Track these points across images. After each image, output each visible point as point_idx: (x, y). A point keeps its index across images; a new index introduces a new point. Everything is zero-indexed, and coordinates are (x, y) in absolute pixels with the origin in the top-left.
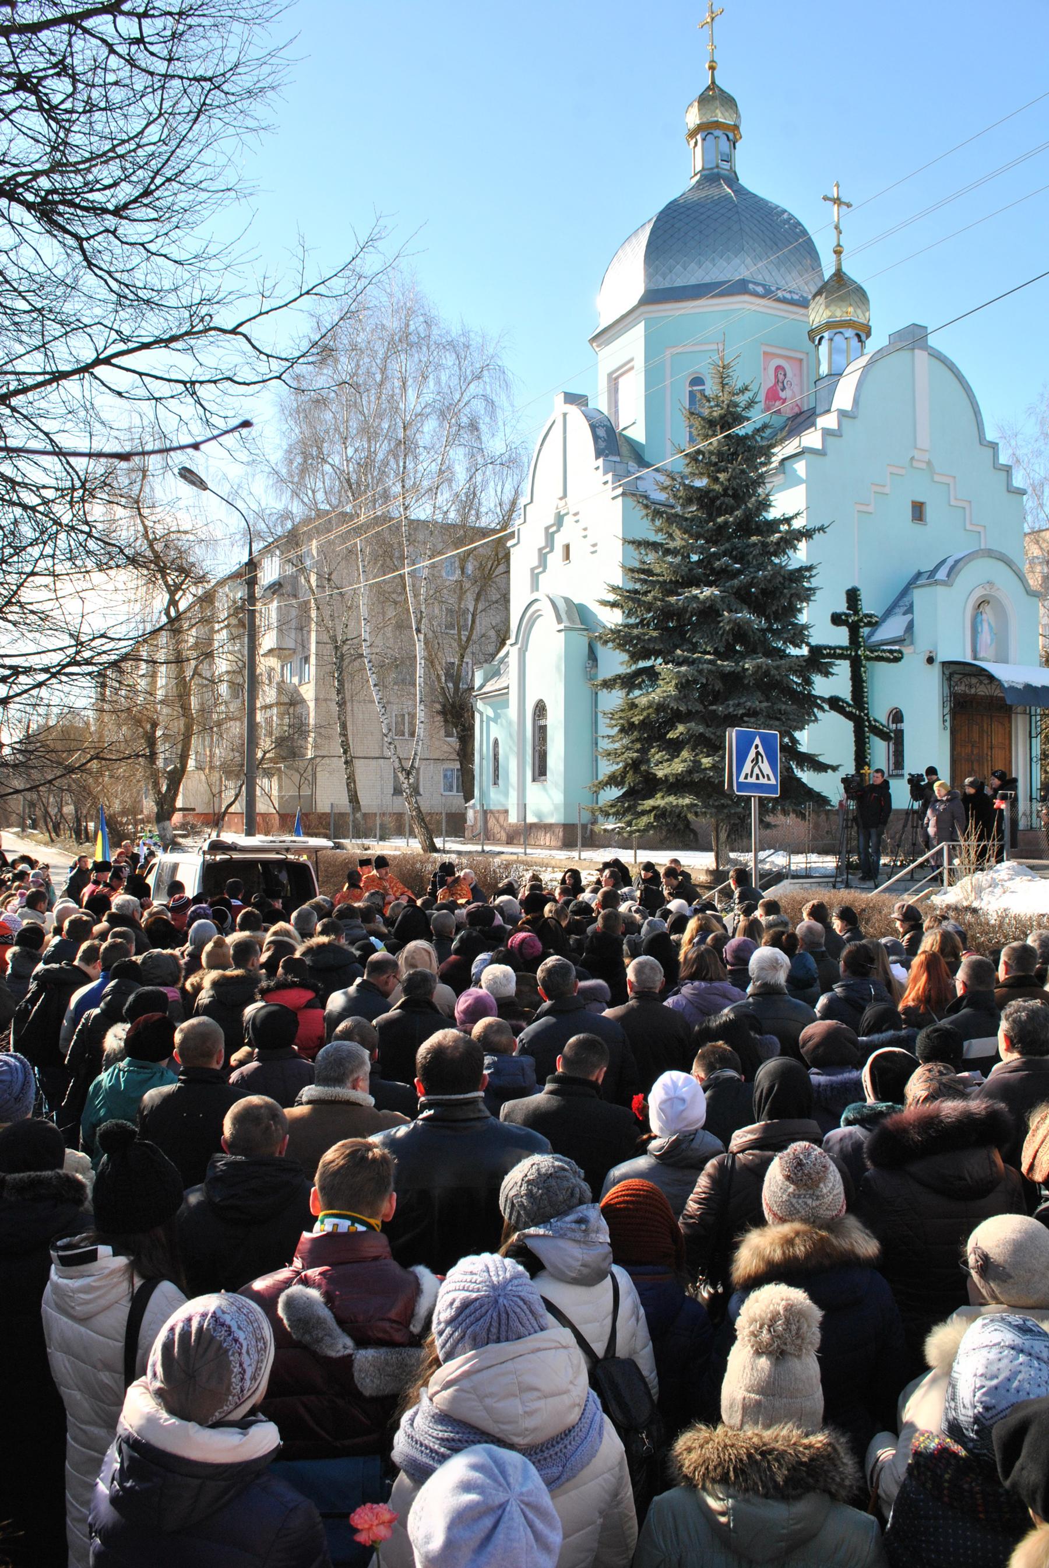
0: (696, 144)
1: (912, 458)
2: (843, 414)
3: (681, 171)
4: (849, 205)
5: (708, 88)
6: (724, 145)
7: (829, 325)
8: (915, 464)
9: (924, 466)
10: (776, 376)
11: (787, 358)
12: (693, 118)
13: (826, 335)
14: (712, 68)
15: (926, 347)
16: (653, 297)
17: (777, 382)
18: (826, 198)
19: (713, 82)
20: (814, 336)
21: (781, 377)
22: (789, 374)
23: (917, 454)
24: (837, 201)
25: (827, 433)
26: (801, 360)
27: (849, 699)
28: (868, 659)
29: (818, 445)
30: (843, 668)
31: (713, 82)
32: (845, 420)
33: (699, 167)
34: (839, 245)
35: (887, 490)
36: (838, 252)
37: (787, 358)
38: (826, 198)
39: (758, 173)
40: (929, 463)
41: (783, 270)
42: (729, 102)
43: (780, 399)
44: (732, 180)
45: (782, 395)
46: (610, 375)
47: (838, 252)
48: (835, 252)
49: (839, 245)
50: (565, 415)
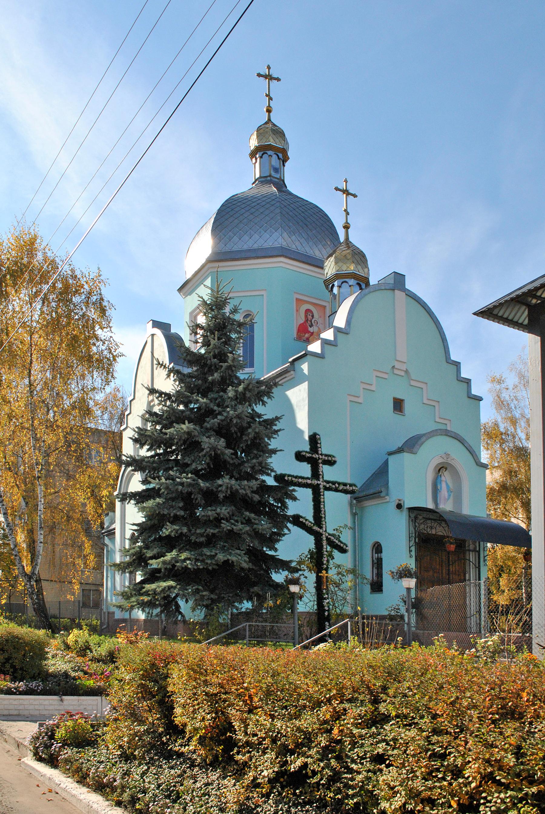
0: (256, 159)
1: (393, 367)
2: (338, 330)
3: (244, 177)
4: (355, 196)
5: (266, 123)
6: (275, 161)
7: (337, 276)
8: (396, 372)
9: (403, 373)
10: (306, 317)
11: (314, 304)
12: (254, 143)
13: (336, 283)
14: (269, 111)
15: (403, 289)
16: (219, 257)
17: (307, 320)
18: (337, 189)
19: (269, 120)
20: (328, 284)
21: (310, 317)
22: (316, 315)
23: (397, 365)
24: (346, 192)
25: (325, 342)
26: (325, 307)
27: (311, 519)
28: (326, 489)
29: (318, 351)
30: (305, 495)
31: (269, 120)
32: (339, 335)
33: (258, 176)
34: (347, 222)
35: (373, 388)
36: (347, 227)
37: (314, 304)
38: (337, 189)
39: (300, 181)
40: (407, 372)
41: (311, 243)
42: (279, 133)
43: (309, 332)
44: (281, 185)
45: (311, 329)
46: (191, 313)
47: (347, 227)
48: (344, 227)
49: (347, 222)
50: (153, 335)
